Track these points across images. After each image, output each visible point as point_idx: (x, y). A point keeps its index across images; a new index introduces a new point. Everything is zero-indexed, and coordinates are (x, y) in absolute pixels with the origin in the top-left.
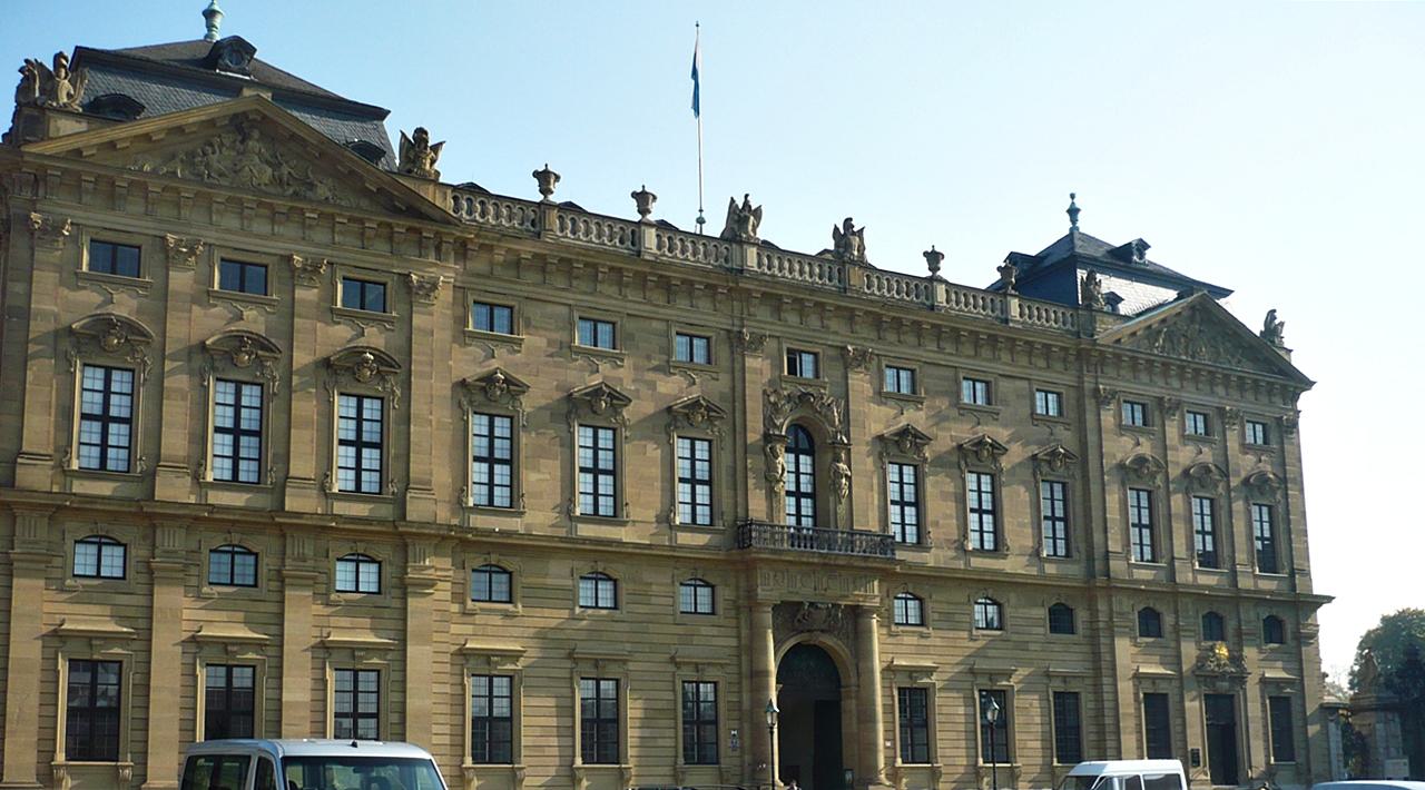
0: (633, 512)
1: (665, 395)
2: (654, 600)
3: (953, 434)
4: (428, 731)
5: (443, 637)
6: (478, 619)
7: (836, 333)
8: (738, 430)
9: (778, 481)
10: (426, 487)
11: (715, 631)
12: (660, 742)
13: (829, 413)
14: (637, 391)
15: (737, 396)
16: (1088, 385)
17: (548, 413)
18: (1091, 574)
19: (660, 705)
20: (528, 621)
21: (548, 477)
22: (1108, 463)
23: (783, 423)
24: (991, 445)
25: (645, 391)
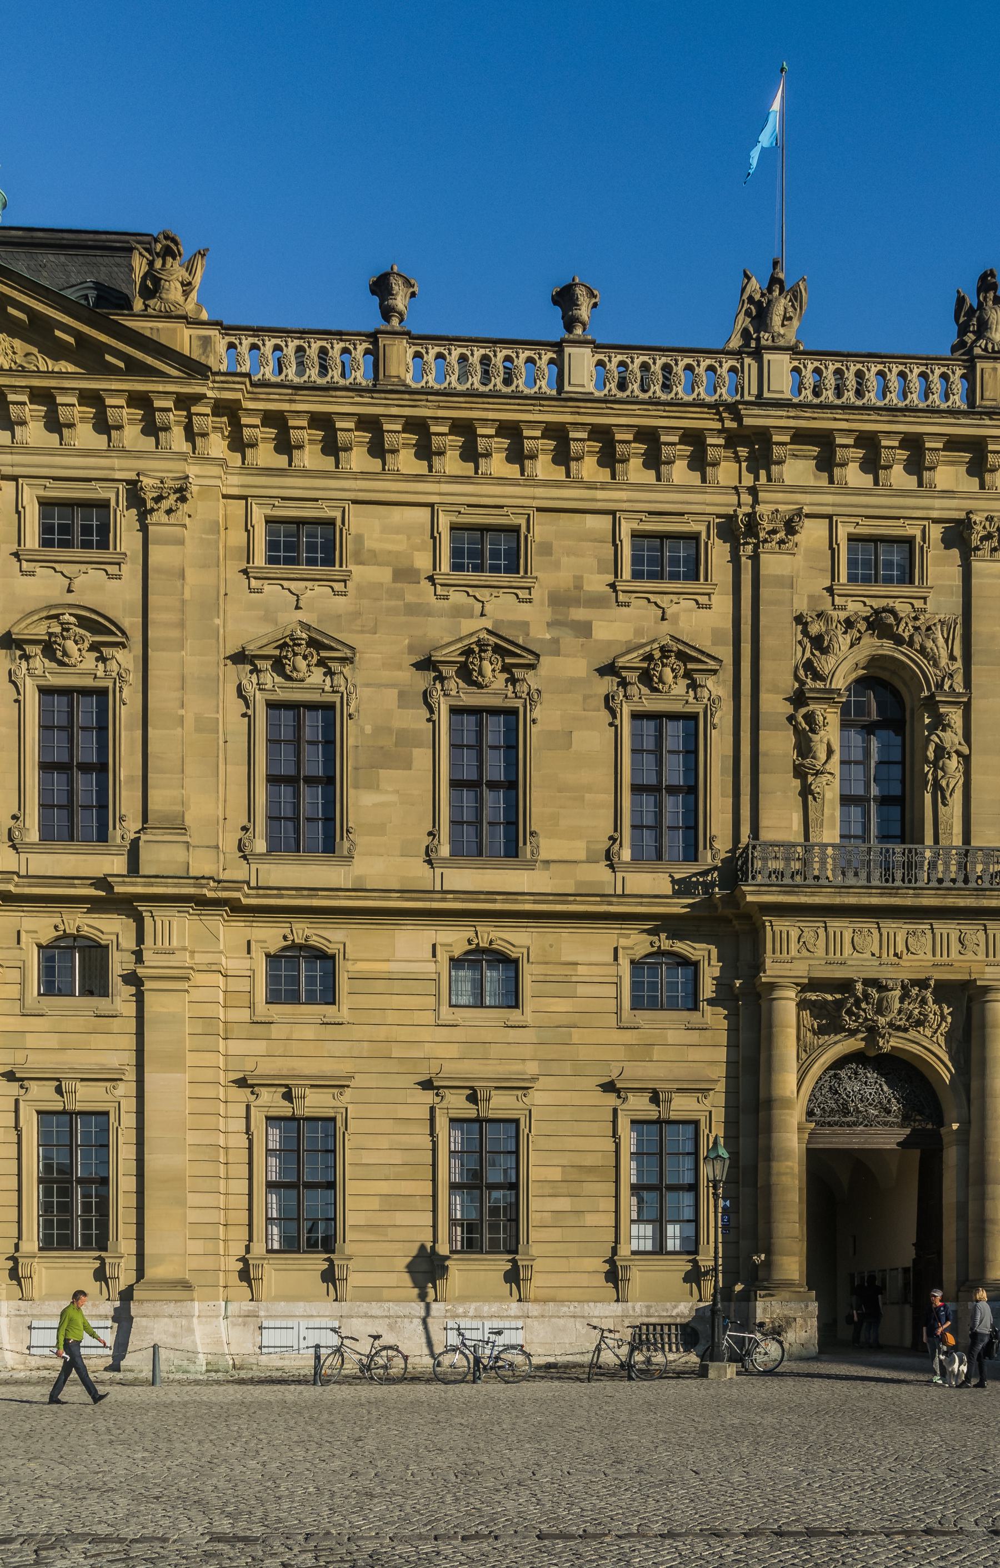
0: (548, 848)
1: (610, 643)
2: (581, 990)
4: (182, 1203)
5: (209, 1058)
6: (275, 1031)
7: (948, 494)
8: (748, 692)
9: (818, 773)
11: (694, 1037)
12: (590, 1219)
13: (929, 644)
14: (556, 641)
15: (747, 632)
19: (589, 1161)
20: (358, 1032)
21: (394, 798)
23: (844, 665)
25: (569, 640)
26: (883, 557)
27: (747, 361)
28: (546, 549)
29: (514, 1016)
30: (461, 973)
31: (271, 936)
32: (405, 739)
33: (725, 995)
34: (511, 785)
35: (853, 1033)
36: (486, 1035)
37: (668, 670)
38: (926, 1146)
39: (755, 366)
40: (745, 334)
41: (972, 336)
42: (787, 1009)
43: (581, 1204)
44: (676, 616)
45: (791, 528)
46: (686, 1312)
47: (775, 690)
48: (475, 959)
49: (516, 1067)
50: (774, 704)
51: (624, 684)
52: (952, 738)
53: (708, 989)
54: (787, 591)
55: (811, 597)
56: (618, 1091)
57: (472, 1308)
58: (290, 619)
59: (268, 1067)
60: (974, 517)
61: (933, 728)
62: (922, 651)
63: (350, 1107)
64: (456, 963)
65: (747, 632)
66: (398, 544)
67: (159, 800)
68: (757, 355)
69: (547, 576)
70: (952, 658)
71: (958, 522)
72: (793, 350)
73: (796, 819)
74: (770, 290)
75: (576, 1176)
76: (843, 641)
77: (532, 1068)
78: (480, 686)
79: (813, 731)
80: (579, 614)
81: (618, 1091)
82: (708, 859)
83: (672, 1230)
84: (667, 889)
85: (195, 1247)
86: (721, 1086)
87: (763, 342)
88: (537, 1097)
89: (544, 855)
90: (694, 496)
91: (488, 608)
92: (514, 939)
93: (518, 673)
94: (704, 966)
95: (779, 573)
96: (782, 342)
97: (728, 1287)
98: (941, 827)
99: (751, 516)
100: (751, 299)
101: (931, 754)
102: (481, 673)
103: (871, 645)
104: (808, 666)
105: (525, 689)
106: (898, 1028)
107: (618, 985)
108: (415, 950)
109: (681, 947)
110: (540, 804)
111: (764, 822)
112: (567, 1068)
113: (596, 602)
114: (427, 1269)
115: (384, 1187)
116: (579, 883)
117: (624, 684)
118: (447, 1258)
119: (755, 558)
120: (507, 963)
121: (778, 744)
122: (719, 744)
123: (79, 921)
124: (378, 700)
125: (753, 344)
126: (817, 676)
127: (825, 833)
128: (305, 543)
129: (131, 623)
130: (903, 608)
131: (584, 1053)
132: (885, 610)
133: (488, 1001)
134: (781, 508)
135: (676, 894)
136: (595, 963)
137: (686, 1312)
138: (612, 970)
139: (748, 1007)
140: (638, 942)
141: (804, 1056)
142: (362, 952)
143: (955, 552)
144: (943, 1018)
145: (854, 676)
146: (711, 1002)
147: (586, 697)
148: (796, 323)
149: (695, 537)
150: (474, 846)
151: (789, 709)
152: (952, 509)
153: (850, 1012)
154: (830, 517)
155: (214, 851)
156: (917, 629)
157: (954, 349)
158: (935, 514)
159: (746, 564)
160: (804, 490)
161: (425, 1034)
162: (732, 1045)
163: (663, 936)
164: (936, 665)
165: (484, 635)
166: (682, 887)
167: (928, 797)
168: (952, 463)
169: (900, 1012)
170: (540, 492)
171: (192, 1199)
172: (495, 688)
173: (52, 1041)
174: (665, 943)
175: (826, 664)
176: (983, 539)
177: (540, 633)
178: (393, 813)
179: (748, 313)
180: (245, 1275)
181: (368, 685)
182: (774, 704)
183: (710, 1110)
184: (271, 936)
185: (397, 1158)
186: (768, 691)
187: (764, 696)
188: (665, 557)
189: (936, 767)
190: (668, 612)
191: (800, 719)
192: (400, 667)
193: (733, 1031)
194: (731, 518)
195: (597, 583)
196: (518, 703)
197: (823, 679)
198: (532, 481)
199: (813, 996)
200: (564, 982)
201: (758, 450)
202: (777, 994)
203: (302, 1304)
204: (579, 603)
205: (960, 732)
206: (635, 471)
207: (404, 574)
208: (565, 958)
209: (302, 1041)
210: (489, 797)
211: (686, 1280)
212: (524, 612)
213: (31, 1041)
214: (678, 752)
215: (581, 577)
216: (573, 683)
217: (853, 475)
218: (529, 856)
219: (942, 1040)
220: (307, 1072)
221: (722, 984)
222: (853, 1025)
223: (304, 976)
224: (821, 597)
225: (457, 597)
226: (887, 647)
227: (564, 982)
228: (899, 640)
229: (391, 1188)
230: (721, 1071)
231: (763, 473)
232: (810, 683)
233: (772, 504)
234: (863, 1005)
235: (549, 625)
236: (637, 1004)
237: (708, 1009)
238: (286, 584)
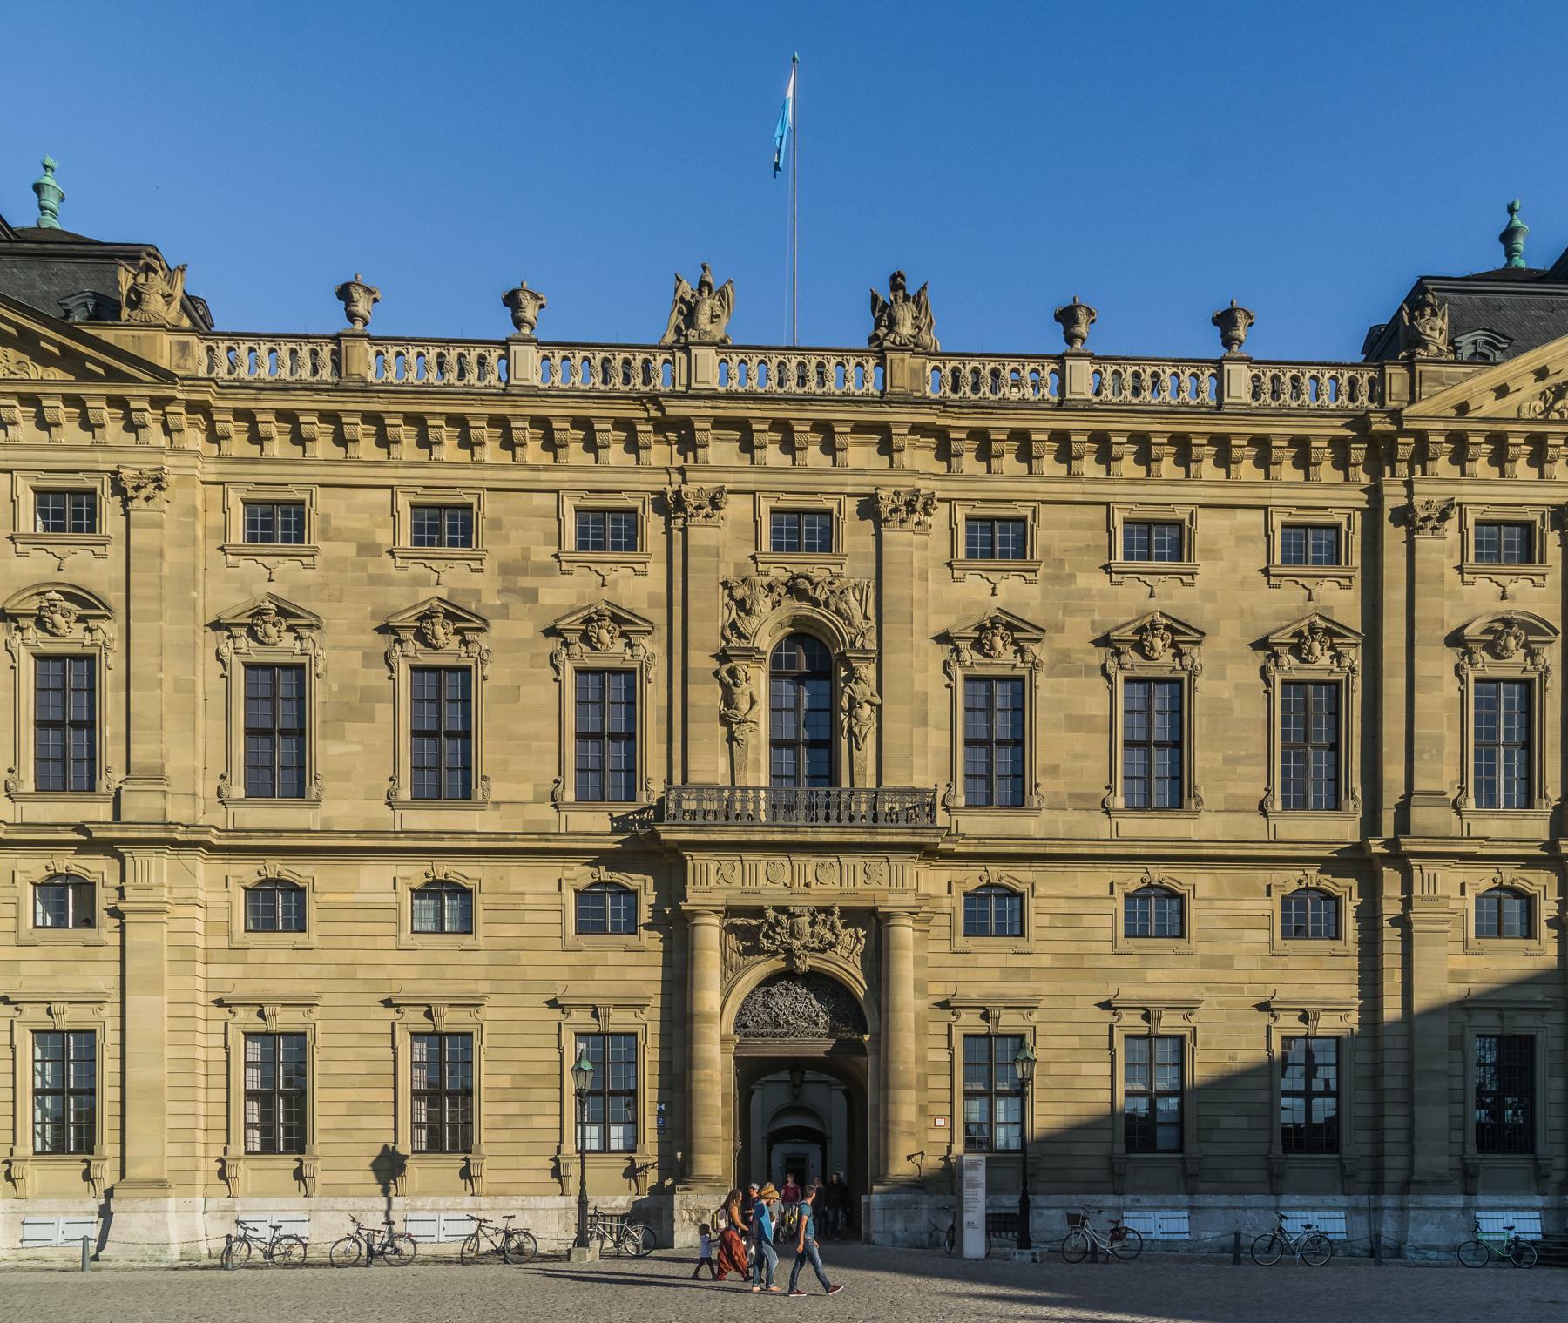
0: (498, 791)
1: (554, 607)
2: (529, 917)
3: (1097, 617)
4: (162, 1111)
6: (252, 956)
7: (858, 471)
9: (740, 722)
10: (157, 776)
11: (632, 958)
12: (537, 1122)
13: (843, 606)
14: (505, 606)
16: (1394, 495)
17: (359, 653)
20: (326, 956)
21: (358, 748)
23: (767, 627)
24: (1167, 627)
25: (517, 606)
26: (804, 529)
27: (679, 354)
28: (496, 524)
29: (467, 940)
30: (424, 902)
31: (248, 871)
32: (369, 695)
34: (465, 735)
35: (774, 954)
36: (443, 958)
37: (604, 631)
39: (684, 357)
40: (678, 330)
41: (885, 330)
42: (710, 933)
43: (529, 1108)
44: (615, 583)
45: (715, 505)
46: (624, 1204)
47: (702, 648)
48: (432, 890)
49: (470, 986)
50: (702, 661)
51: (566, 644)
52: (864, 690)
53: (645, 915)
54: (713, 560)
55: (737, 565)
56: (561, 1007)
57: (429, 1201)
58: (262, 589)
59: (244, 989)
60: (882, 493)
61: (847, 680)
62: (838, 611)
63: (319, 1023)
64: (418, 893)
65: (677, 597)
66: (361, 522)
67: (140, 753)
68: (686, 349)
69: (494, 548)
70: (866, 618)
71: (871, 495)
72: (721, 345)
73: (723, 764)
74: (700, 293)
75: (524, 1084)
76: (764, 604)
77: (484, 987)
78: (435, 648)
79: (735, 684)
80: (526, 582)
81: (561, 1007)
82: (643, 799)
83: (616, 1131)
84: (606, 826)
85: (172, 1149)
86: (656, 1002)
87: (691, 339)
88: (488, 1013)
89: (494, 797)
90: (630, 474)
91: (443, 577)
92: (301, 871)
93: (469, 636)
94: (641, 894)
95: (705, 543)
96: (707, 339)
97: (661, 1182)
98: (856, 769)
99: (678, 493)
100: (682, 300)
101: (845, 703)
102: (434, 637)
103: (791, 606)
104: (733, 626)
105: (477, 649)
106: (813, 949)
107: (562, 912)
108: (378, 881)
109: (618, 877)
110: (489, 752)
111: (692, 766)
112: (516, 987)
113: (542, 570)
114: (389, 1167)
115: (351, 1095)
116: (526, 822)
117: (566, 644)
118: (406, 1157)
119: (684, 530)
120: (463, 893)
121: (706, 696)
122: (653, 698)
123: (67, 862)
124: (341, 662)
125: (682, 340)
126: (741, 636)
127: (749, 775)
128: (277, 522)
129: (115, 598)
130: (818, 573)
131: (531, 973)
132: (799, 576)
133: (447, 927)
134: (705, 486)
135: (615, 831)
136: (542, 895)
137: (624, 1204)
138: (557, 899)
139: (677, 930)
140: (581, 874)
141: (730, 974)
142: (327, 884)
143: (870, 523)
144: (858, 940)
145: (781, 634)
146: (647, 927)
147: (533, 656)
148: (725, 320)
149: (634, 511)
150: (434, 790)
151: (715, 665)
152: (864, 485)
153: (767, 936)
154: (753, 493)
155: (189, 799)
156: (832, 592)
157: (871, 340)
158: (849, 490)
159: (678, 535)
160: (727, 469)
161: (387, 958)
162: (667, 965)
163: (602, 868)
164: (850, 624)
165: (436, 603)
166: (620, 825)
167: (844, 742)
168: (864, 444)
169: (812, 935)
170: (489, 474)
171: (171, 1107)
172: (449, 650)
173: (45, 968)
174: (605, 876)
175: (749, 624)
176: (891, 511)
177: (491, 599)
178: (358, 762)
179: (681, 312)
180: (222, 1174)
181: (335, 648)
182: (702, 661)
183: (648, 1024)
184: (248, 871)
185: (362, 1068)
186: (696, 649)
187: (691, 654)
188: (607, 530)
189: (851, 716)
190: (608, 579)
191: (724, 674)
192: (363, 631)
193: (667, 952)
194: (663, 494)
195: (543, 554)
196: (471, 662)
197: (746, 638)
198: (479, 465)
199: (738, 921)
200: (513, 909)
201: (684, 435)
202: (698, 920)
203: (274, 1199)
205: (874, 683)
206: (575, 453)
207: (368, 549)
208: (514, 889)
209: (277, 963)
211: (625, 1175)
212: (476, 580)
213: (25, 968)
214: (620, 703)
215: (528, 549)
216: (521, 644)
217: (773, 455)
218: (480, 798)
219: (858, 960)
220: (279, 992)
221: (656, 910)
222: (773, 947)
223: (277, 907)
224: (746, 564)
225: (415, 568)
226: (806, 609)
227: (513, 909)
228: (816, 603)
229: (358, 1097)
230: (658, 988)
231: (690, 455)
232: (735, 642)
233: (697, 485)
234: (778, 930)
235: (499, 592)
236: (582, 929)
237: (644, 933)
238: (259, 559)
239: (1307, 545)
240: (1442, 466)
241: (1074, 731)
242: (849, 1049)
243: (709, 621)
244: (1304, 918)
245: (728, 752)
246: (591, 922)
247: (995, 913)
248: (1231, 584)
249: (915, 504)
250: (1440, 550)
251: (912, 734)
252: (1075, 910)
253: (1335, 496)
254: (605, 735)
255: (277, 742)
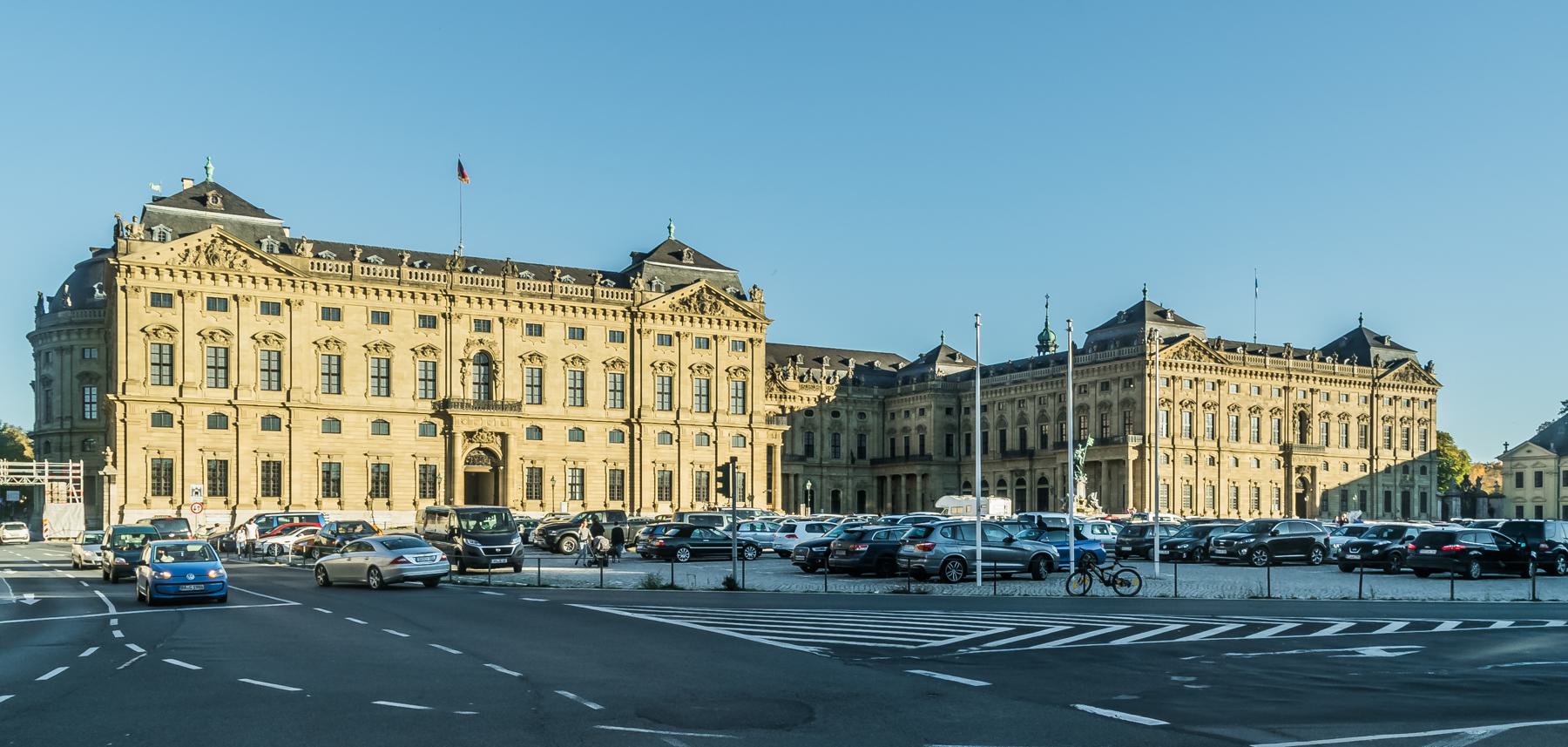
15: (449, 343)
16: (637, 326)
18: (632, 415)
22: (646, 365)
23: (474, 351)
26: (484, 326)
33: (443, 433)
38: (495, 470)
53: (439, 430)
139: (449, 434)
188: (428, 322)
204: (404, 333)
210: (383, 380)
239: (616, 337)
240: (649, 320)
241: (557, 383)
242: (495, 470)
243: (459, 353)
244: (616, 437)
245: (462, 386)
246: (423, 434)
247: (536, 433)
248: (598, 348)
249: (514, 321)
250: (649, 342)
251: (511, 385)
252: (556, 434)
253: (623, 325)
254: (430, 378)
255: (334, 376)
